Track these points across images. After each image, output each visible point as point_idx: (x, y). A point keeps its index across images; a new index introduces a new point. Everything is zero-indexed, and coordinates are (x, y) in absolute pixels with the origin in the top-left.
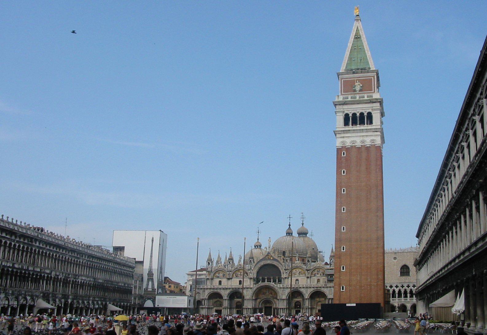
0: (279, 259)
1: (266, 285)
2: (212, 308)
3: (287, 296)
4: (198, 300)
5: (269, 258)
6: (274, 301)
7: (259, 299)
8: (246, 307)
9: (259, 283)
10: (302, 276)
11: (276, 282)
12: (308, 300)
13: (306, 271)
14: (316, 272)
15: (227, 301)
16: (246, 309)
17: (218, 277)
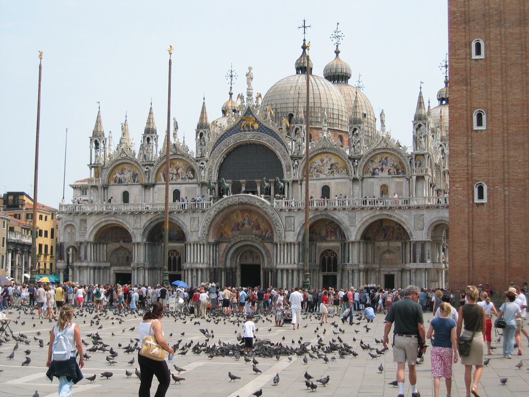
0: (276, 130)
1: (241, 203)
2: (106, 268)
3: (299, 234)
4: (69, 245)
5: (250, 128)
6: (264, 247)
9: (225, 196)
10: (339, 177)
11: (270, 194)
12: (356, 246)
13: (351, 163)
14: (376, 164)
15: (142, 249)
16: (192, 270)
17: (120, 181)
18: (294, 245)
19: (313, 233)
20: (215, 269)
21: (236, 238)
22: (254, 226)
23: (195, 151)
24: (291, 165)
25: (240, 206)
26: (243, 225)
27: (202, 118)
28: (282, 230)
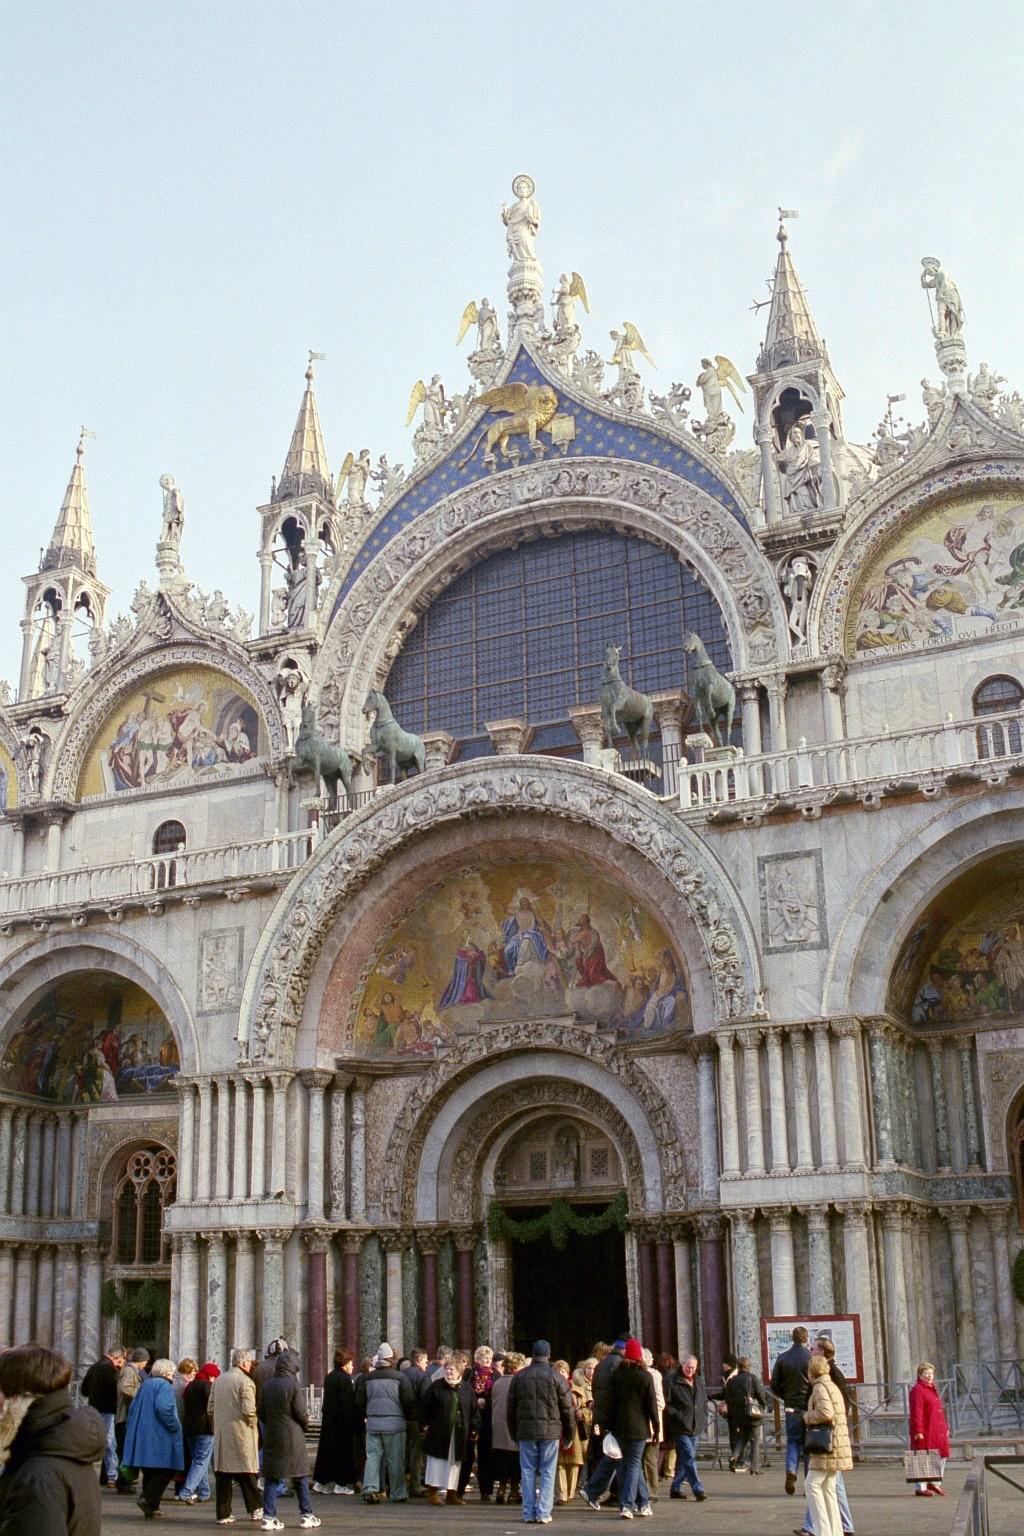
1: (479, 816)
3: (862, 964)
5: (529, 447)
6: (635, 1084)
7: (398, 1071)
8: (200, 1220)
16: (201, 1244)
18: (833, 1037)
19: (945, 974)
20: (339, 1239)
21: (463, 1041)
22: (571, 963)
23: (253, 608)
24: (772, 588)
25: (477, 836)
26: (507, 963)
27: (295, 454)
28: (742, 949)
